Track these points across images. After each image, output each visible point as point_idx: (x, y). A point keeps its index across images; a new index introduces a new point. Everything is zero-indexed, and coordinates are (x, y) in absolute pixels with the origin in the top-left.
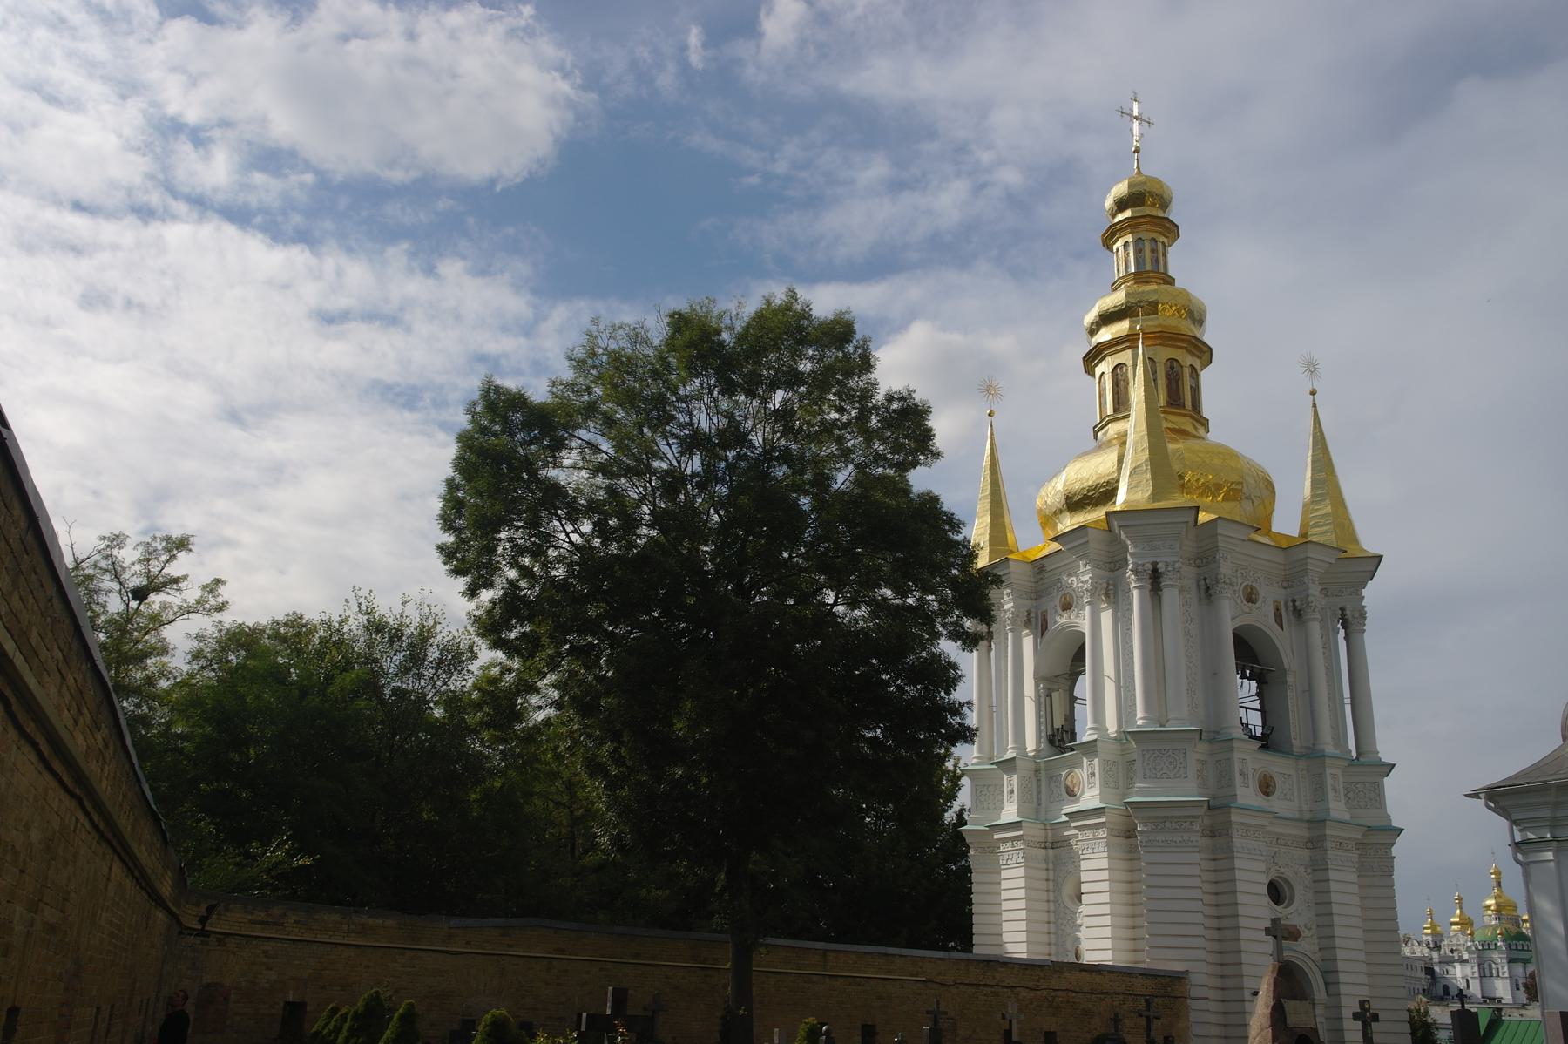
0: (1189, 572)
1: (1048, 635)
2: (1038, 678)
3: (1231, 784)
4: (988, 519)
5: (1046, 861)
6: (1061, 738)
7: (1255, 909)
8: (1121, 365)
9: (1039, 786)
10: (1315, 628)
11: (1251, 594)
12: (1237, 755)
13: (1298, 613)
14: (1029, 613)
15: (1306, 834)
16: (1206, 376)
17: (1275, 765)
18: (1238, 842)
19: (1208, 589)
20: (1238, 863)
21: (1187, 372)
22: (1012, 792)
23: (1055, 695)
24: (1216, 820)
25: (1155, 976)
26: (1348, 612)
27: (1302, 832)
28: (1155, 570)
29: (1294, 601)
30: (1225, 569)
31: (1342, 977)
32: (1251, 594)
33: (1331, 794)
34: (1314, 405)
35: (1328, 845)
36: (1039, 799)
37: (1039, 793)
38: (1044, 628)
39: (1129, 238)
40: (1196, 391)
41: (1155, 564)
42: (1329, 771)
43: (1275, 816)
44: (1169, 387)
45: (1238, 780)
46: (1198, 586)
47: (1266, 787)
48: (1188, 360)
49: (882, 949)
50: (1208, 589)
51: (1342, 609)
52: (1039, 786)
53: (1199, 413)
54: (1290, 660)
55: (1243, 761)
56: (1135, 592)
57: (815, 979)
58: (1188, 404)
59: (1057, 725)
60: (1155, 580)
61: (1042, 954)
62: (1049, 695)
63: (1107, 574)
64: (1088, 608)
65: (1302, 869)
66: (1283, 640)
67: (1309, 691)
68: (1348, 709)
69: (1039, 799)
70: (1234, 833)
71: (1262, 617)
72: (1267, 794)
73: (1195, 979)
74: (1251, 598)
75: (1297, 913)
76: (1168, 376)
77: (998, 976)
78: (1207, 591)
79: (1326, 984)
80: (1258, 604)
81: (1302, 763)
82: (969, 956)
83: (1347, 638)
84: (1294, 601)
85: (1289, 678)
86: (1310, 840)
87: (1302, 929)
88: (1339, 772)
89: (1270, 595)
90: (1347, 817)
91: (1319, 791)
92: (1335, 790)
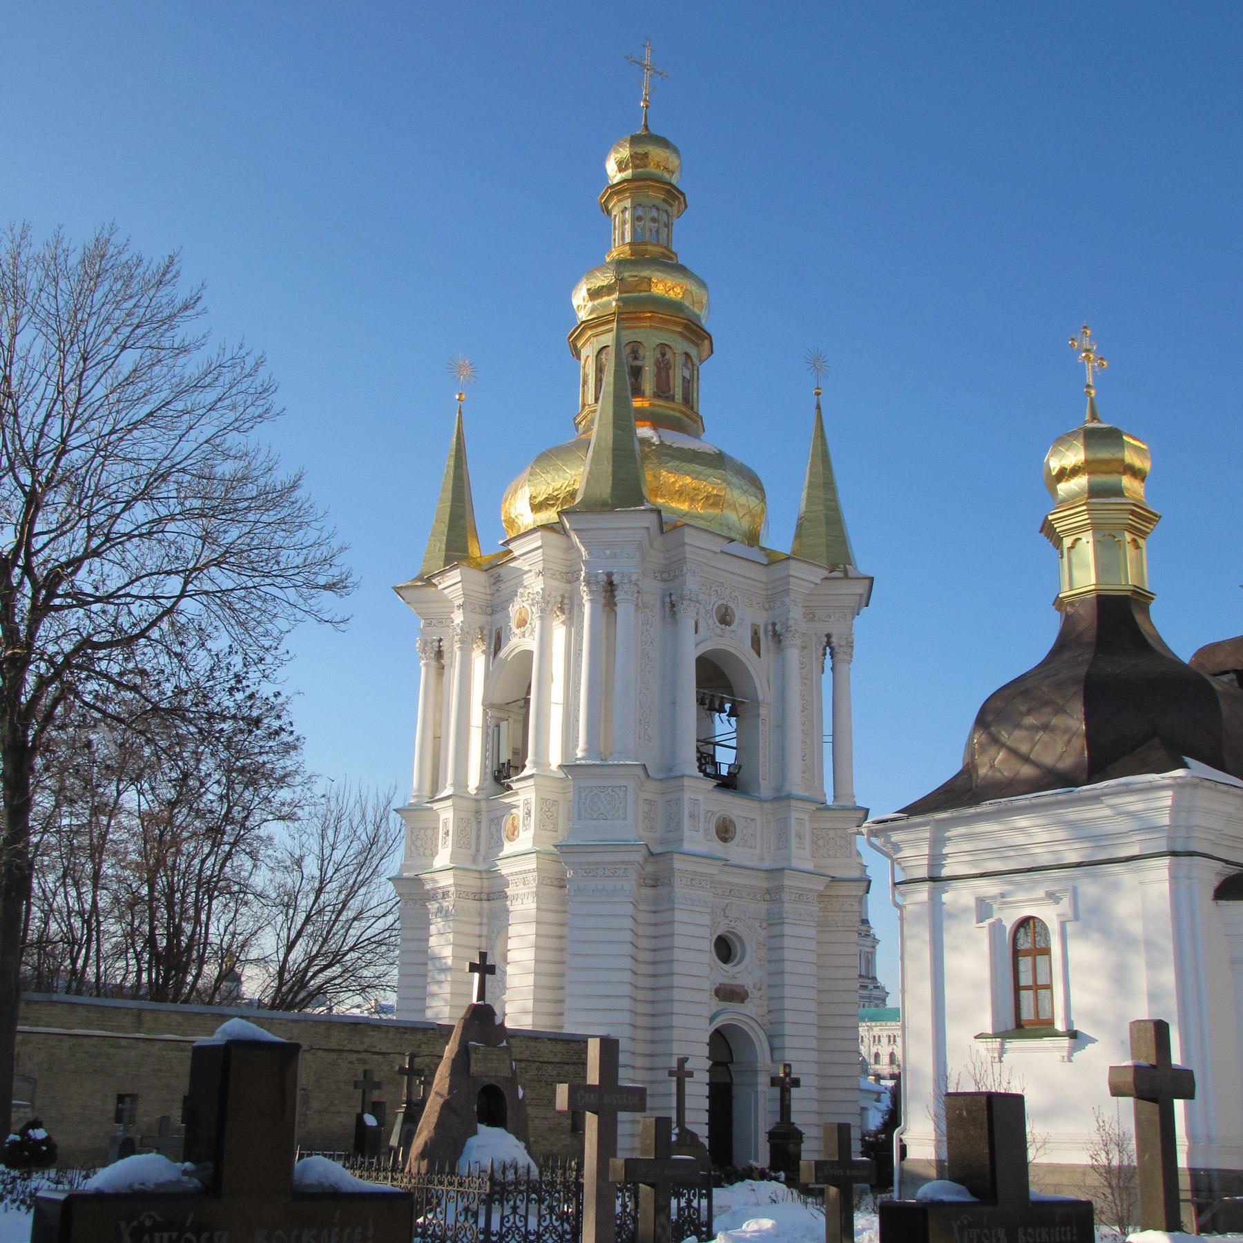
0: (653, 589)
2: (488, 705)
3: (678, 826)
6: (502, 774)
7: (696, 968)
9: (479, 830)
10: (793, 655)
11: (726, 614)
12: (687, 795)
13: (777, 637)
15: (764, 885)
16: (706, 370)
17: (730, 805)
20: (678, 916)
21: (680, 360)
22: (447, 833)
23: (503, 725)
24: (657, 870)
27: (761, 883)
28: (611, 583)
29: (774, 625)
30: (692, 584)
31: (788, 1041)
32: (726, 614)
33: (794, 841)
34: (818, 407)
35: (786, 896)
36: (478, 844)
37: (478, 837)
38: (498, 648)
39: (628, 203)
40: (688, 384)
41: (609, 575)
42: (794, 815)
43: (726, 863)
44: (658, 375)
45: (687, 823)
46: (663, 603)
47: (725, 831)
48: (680, 346)
50: (673, 606)
51: (829, 636)
52: (479, 830)
53: (692, 408)
54: (764, 691)
55: (695, 802)
57: (124, 1043)
58: (679, 396)
59: (504, 760)
60: (609, 590)
61: (545, 1025)
62: (498, 726)
65: (757, 924)
66: (758, 670)
67: (781, 727)
68: (827, 749)
69: (478, 844)
70: (677, 882)
71: (735, 641)
72: (725, 840)
74: (725, 618)
75: (744, 973)
76: (657, 363)
77: (367, 1041)
78: (671, 608)
79: (772, 1049)
80: (733, 627)
81: (767, 806)
83: (832, 669)
84: (774, 625)
85: (763, 711)
86: (768, 891)
88: (806, 817)
90: (809, 866)
91: (783, 835)
92: (799, 836)
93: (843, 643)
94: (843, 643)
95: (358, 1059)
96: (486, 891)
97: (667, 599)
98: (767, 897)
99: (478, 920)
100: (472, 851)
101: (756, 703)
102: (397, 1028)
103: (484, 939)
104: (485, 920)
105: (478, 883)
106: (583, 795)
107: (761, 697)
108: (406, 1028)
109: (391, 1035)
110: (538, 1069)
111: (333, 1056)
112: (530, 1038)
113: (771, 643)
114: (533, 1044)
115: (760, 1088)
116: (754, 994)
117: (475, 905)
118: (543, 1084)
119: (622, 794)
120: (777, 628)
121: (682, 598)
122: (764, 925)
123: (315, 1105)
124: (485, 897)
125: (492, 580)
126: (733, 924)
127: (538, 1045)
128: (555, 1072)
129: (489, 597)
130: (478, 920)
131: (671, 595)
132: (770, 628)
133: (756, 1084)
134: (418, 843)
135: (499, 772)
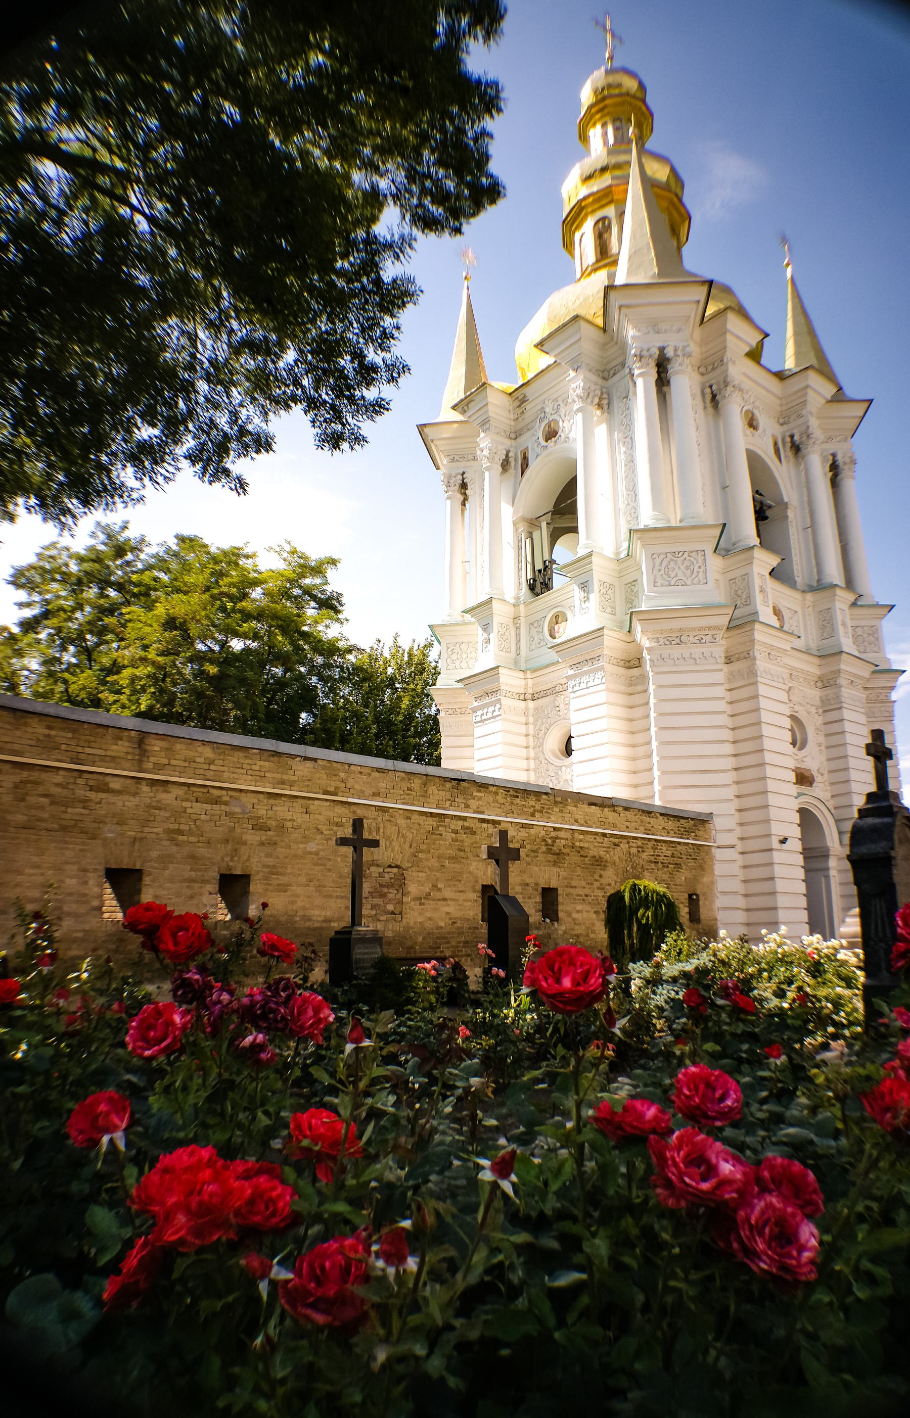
1: (528, 473)
4: (462, 370)
5: (526, 714)
8: (603, 219)
9: (518, 635)
13: (796, 449)
14: (508, 452)
18: (761, 664)
19: (714, 397)
25: (678, 818)
26: (839, 457)
29: (792, 436)
33: (841, 630)
35: (842, 681)
36: (518, 648)
37: (518, 641)
41: (662, 349)
46: (703, 394)
49: (269, 744)
52: (518, 635)
56: (640, 382)
63: (600, 381)
64: (580, 415)
65: (813, 710)
67: (813, 526)
69: (518, 648)
73: (719, 823)
77: (473, 803)
81: (809, 597)
82: (432, 770)
85: (790, 513)
86: (820, 679)
87: (815, 774)
89: (769, 428)
92: (844, 624)
93: (848, 461)
94: (848, 461)
95: (463, 827)
96: (530, 691)
97: (708, 390)
98: (820, 684)
99: (524, 720)
100: (513, 655)
101: (786, 506)
102: (507, 789)
103: (531, 738)
104: (531, 720)
105: (523, 682)
106: (658, 561)
107: (786, 500)
108: (516, 790)
109: (499, 798)
110: (654, 848)
111: (431, 821)
112: (643, 811)
113: (790, 454)
114: (647, 819)
115: (833, 873)
116: (818, 778)
117: (523, 703)
118: (660, 866)
119: (700, 559)
120: (796, 438)
121: (726, 384)
122: (821, 711)
123: (413, 888)
124: (529, 696)
125: (517, 403)
126: (797, 708)
127: (652, 820)
128: (669, 853)
129: (513, 423)
130: (524, 720)
131: (711, 387)
132: (788, 439)
133: (828, 869)
134: (454, 657)
135: (534, 580)
